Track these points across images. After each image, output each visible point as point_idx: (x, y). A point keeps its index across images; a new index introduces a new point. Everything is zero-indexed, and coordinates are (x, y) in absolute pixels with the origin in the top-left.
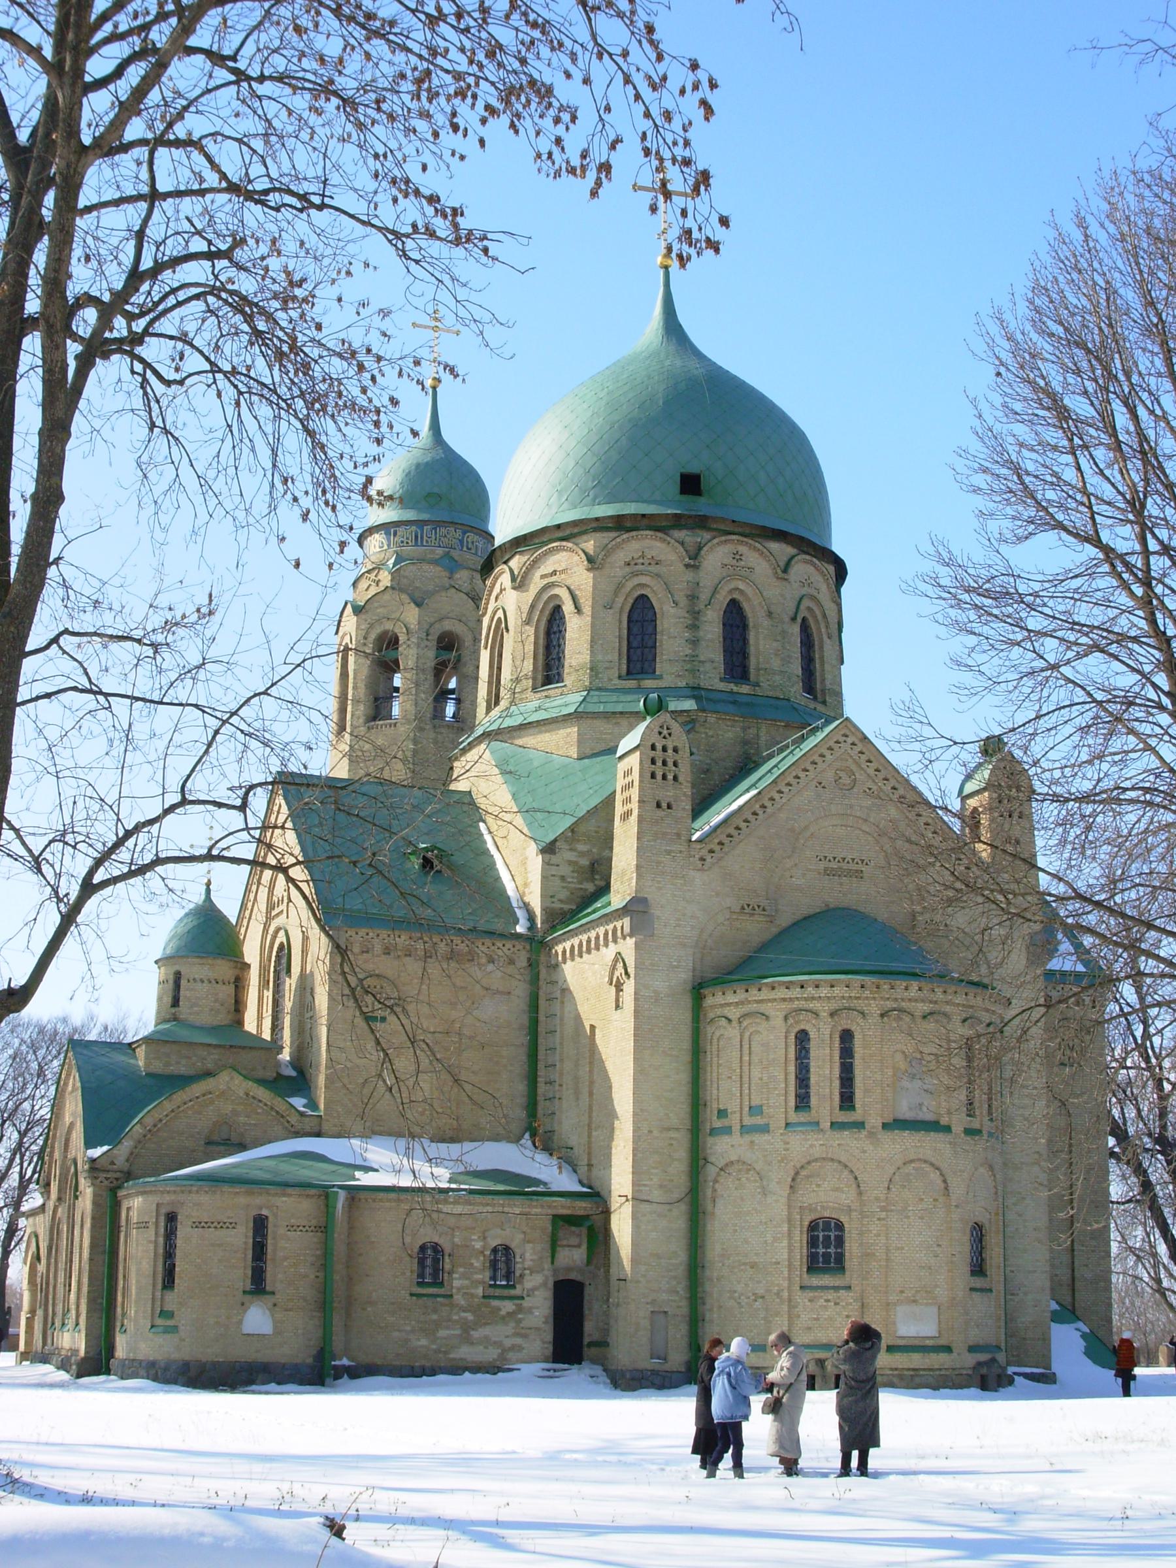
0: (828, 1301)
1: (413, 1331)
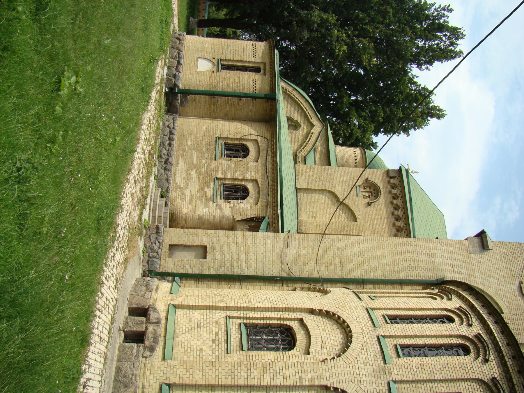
0: (217, 334)
1: (196, 138)
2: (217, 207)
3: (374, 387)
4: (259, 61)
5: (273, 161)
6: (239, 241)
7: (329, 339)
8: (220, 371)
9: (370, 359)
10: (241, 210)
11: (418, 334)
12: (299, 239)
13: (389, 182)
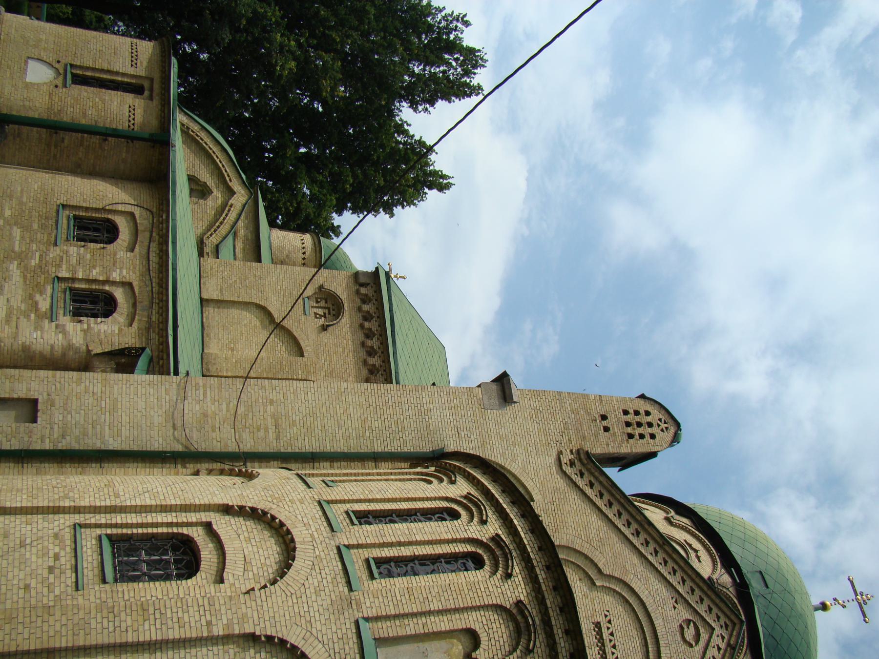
0: (57, 557)
1: (21, 203)
2: (59, 330)
3: (334, 629)
4: (143, 73)
5: (161, 251)
6: (98, 389)
7: (256, 554)
8: (64, 621)
9: (326, 584)
10: (103, 336)
11: (402, 540)
12: (204, 386)
13: (358, 292)
